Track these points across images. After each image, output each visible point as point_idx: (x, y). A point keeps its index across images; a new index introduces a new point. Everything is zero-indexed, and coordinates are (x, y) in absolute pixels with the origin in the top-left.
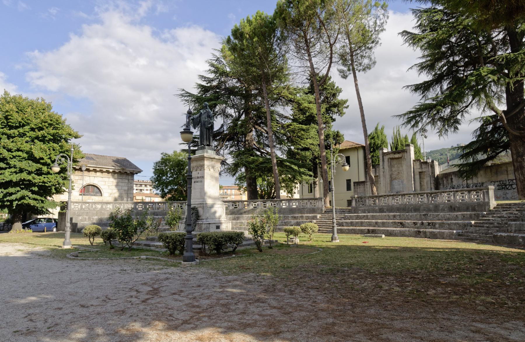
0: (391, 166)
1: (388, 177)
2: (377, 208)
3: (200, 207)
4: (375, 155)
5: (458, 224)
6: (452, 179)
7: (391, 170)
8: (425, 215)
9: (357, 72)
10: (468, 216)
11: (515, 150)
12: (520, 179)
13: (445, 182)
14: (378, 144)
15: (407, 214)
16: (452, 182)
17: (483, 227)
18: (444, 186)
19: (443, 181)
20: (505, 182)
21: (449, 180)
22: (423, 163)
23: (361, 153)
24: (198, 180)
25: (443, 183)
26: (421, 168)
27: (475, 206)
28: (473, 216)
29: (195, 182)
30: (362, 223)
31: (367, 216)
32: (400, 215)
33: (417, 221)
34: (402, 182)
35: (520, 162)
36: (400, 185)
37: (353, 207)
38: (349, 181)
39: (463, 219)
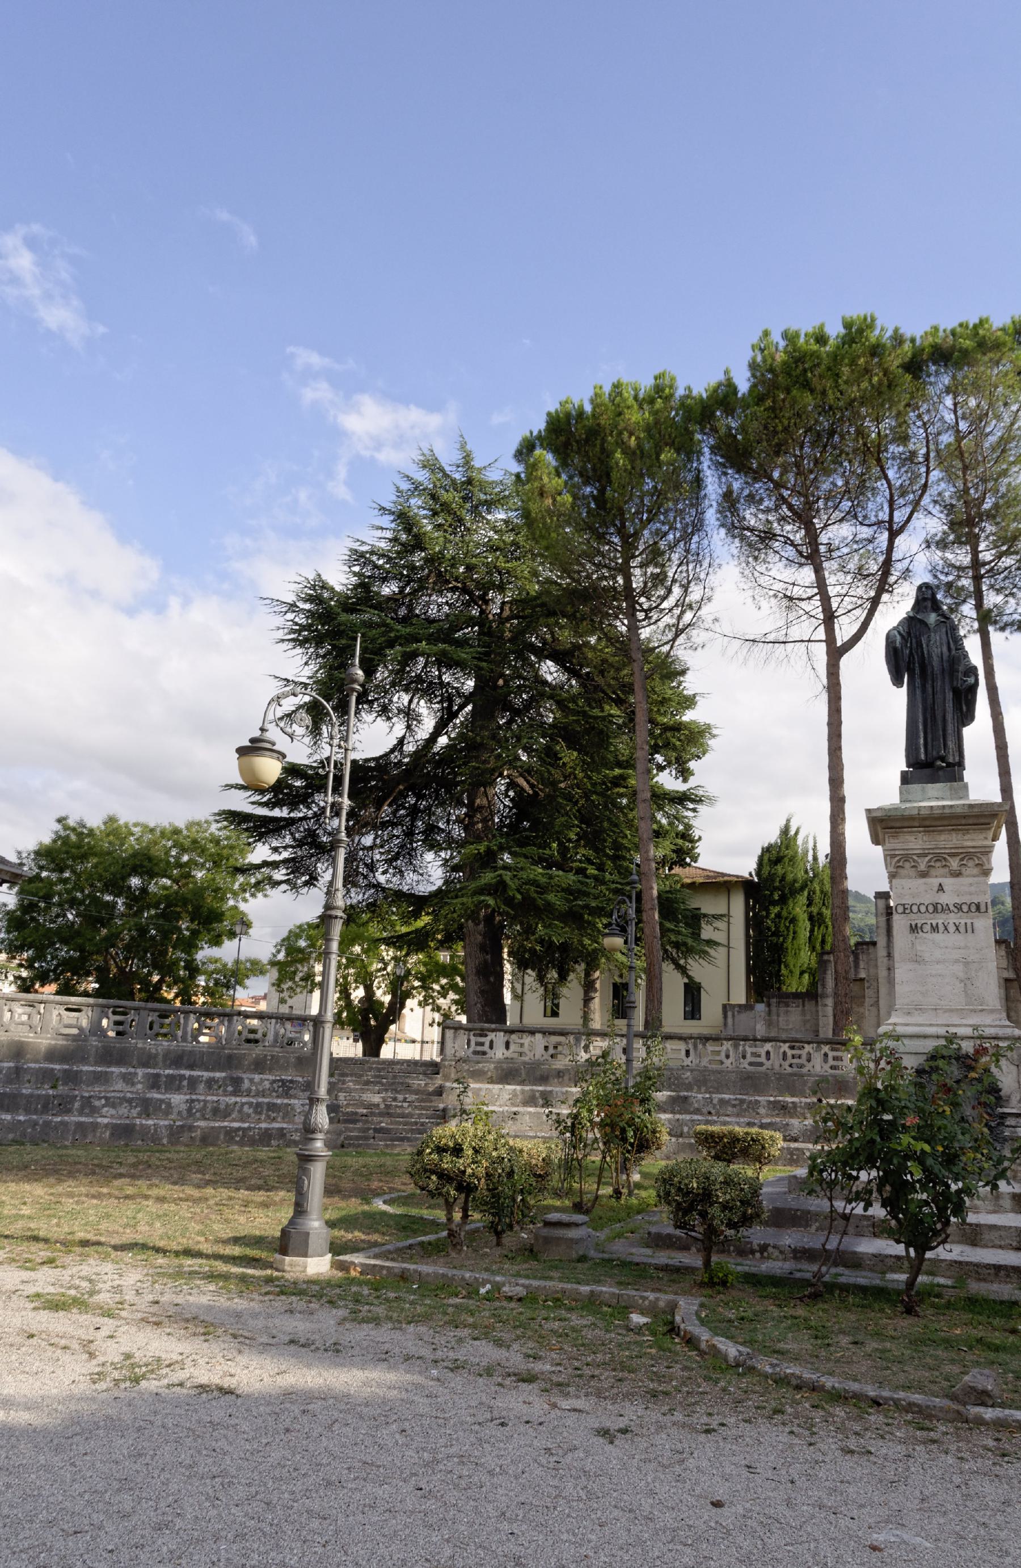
4: (784, 913)
14: (795, 881)
23: (738, 905)
24: (939, 919)
29: (914, 929)
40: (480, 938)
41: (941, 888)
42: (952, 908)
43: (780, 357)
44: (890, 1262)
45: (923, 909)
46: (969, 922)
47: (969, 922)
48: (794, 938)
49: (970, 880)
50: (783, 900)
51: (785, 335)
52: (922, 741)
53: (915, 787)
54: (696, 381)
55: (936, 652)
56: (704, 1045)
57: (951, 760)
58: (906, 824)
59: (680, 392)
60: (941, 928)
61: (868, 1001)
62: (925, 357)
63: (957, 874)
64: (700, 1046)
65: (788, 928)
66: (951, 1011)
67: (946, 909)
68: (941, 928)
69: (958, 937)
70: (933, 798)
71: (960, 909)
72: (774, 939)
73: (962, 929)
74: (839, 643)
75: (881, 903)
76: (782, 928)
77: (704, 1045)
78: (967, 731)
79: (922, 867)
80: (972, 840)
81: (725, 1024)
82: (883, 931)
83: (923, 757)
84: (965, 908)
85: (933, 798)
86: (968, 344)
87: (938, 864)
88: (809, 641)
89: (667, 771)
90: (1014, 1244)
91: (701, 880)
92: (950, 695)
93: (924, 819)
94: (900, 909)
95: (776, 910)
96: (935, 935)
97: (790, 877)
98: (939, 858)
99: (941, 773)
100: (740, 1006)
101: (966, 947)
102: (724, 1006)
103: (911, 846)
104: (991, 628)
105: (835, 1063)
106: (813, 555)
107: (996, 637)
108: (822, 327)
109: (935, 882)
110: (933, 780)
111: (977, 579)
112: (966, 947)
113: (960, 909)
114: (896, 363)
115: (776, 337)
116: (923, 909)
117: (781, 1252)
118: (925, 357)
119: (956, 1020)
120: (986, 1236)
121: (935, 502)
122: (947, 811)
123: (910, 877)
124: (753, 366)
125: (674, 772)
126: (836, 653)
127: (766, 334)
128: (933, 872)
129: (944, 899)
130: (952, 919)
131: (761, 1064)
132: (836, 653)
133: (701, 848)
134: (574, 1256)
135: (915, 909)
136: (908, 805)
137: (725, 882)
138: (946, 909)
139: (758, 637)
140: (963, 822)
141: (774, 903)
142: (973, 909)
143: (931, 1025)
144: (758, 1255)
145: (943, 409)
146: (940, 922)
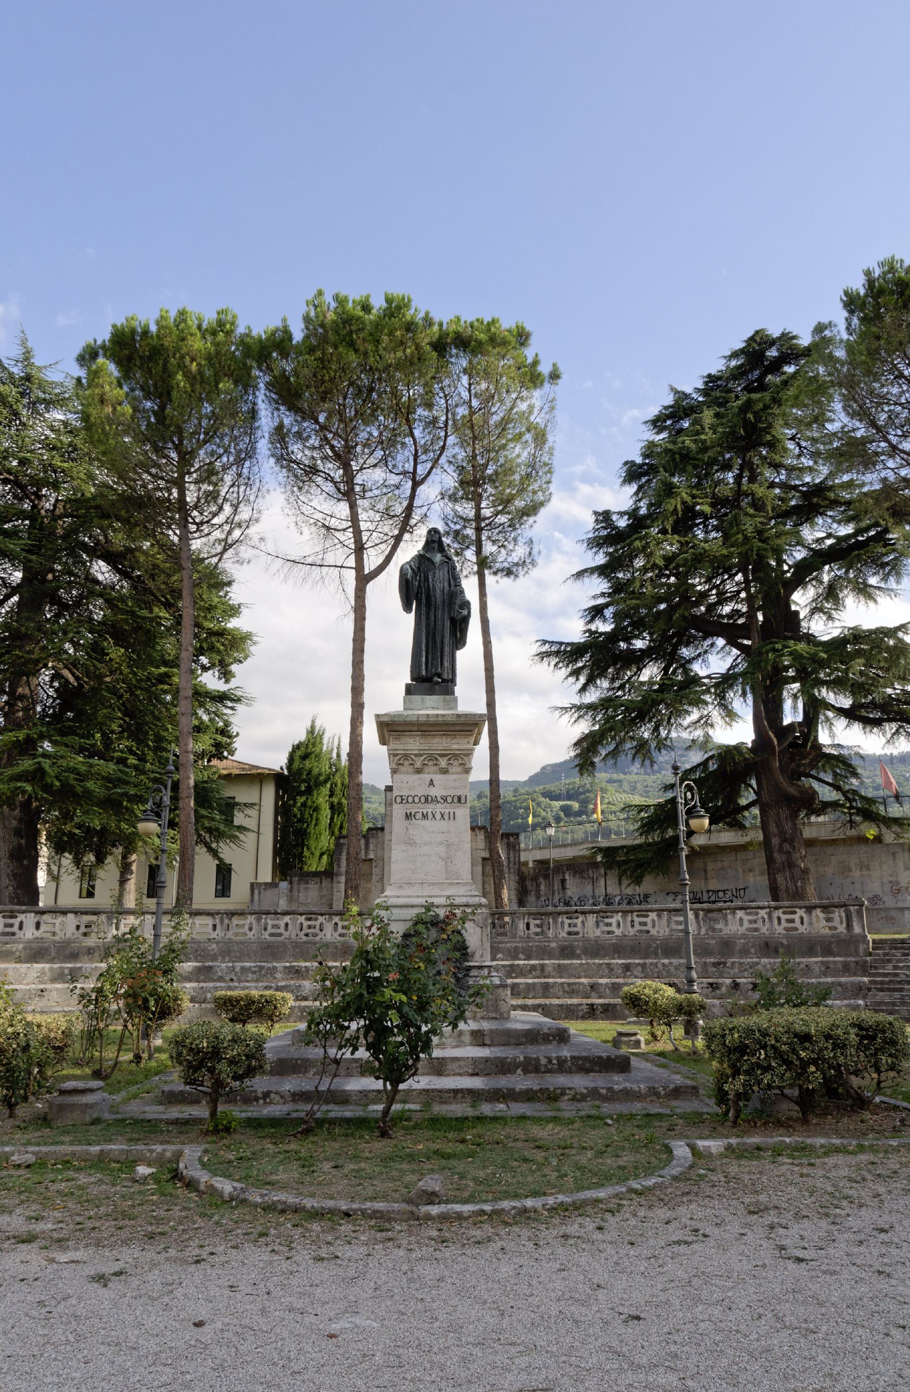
2: (553, 945)
4: (309, 803)
5: (840, 984)
6: (563, 881)
8: (719, 964)
10: (840, 966)
11: (777, 826)
12: (787, 890)
13: (542, 887)
14: (320, 774)
15: (666, 961)
16: (564, 888)
17: (901, 990)
18: (538, 897)
19: (538, 886)
20: (699, 895)
21: (557, 885)
23: (269, 794)
24: (429, 809)
25: (538, 890)
27: (831, 943)
28: (853, 965)
29: (408, 816)
30: (546, 986)
31: (543, 967)
32: (643, 966)
33: (720, 981)
35: (788, 853)
39: (825, 974)
40: (14, 823)
41: (431, 783)
43: (331, 316)
44: (371, 1096)
45: (417, 800)
46: (452, 811)
47: (452, 811)
48: (316, 825)
49: (455, 777)
50: (309, 791)
51: (336, 298)
53: (417, 698)
54: (256, 322)
55: (439, 586)
56: (230, 919)
58: (407, 728)
59: (241, 330)
60: (430, 816)
62: (449, 341)
63: (445, 771)
64: (226, 921)
65: (311, 816)
66: (434, 884)
67: (435, 800)
68: (430, 816)
69: (443, 823)
70: (430, 707)
71: (445, 801)
72: (299, 825)
73: (446, 817)
74: (366, 572)
76: (307, 816)
78: (459, 654)
79: (418, 765)
80: (457, 744)
81: (252, 901)
83: (424, 673)
84: (449, 800)
85: (430, 707)
86: (482, 336)
87: (431, 763)
88: (342, 567)
89: (211, 672)
90: (470, 1071)
92: (448, 624)
93: (423, 725)
94: (399, 800)
95: (303, 799)
96: (425, 822)
97: (316, 771)
98: (432, 758)
99: (437, 687)
100: (266, 884)
101: (449, 832)
102: (252, 885)
103: (410, 747)
104: (486, 572)
105: (344, 931)
106: (348, 492)
107: (490, 579)
108: (368, 298)
109: (427, 777)
110: (431, 693)
111: (479, 530)
112: (449, 832)
113: (445, 801)
114: (427, 340)
115: (328, 298)
116: (417, 800)
117: (282, 1097)
118: (449, 341)
120: (450, 1066)
121: (450, 462)
122: (440, 719)
123: (408, 773)
124: (307, 319)
125: (217, 674)
126: (363, 579)
127: (320, 293)
128: (426, 769)
129: (433, 792)
130: (439, 808)
131: (280, 935)
132: (363, 579)
133: (238, 744)
134: (88, 1119)
135: (410, 800)
136: (410, 712)
137: (259, 774)
138: (435, 800)
141: (301, 794)
144: (261, 1101)
145: (459, 387)
146: (430, 811)
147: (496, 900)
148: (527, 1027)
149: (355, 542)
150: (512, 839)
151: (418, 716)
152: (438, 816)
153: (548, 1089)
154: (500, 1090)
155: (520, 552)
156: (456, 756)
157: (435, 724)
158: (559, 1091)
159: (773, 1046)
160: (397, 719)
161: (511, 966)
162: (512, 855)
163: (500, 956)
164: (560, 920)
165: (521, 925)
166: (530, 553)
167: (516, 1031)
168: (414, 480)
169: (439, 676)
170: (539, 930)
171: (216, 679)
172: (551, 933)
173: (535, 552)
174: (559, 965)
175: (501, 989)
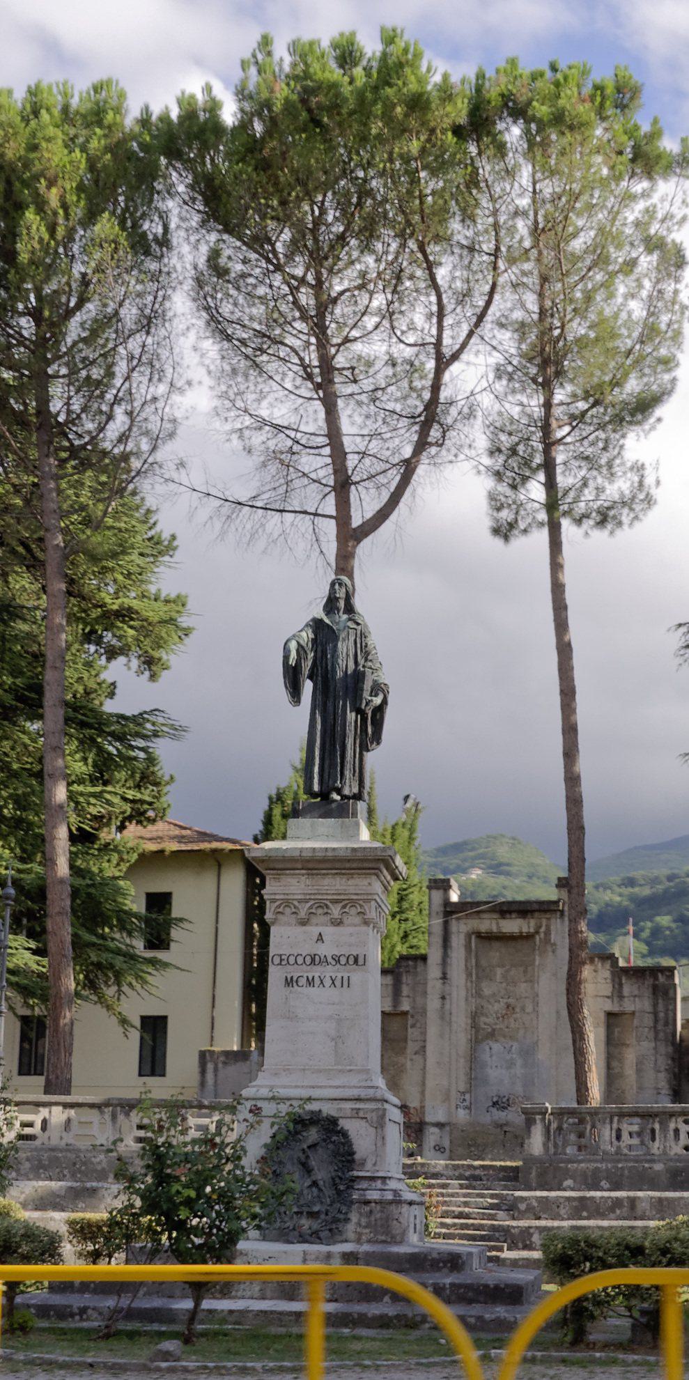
0: (478, 974)
1: (461, 1020)
2: (658, 1167)
3: (356, 1115)
7: (479, 994)
9: (565, 523)
22: (625, 971)
24: (316, 972)
26: (618, 993)
29: (289, 982)
31: (633, 1202)
34: (528, 1053)
36: (510, 1064)
37: (530, 1160)
38: (154, 1027)
41: (320, 938)
42: (330, 959)
43: (282, 92)
45: (300, 960)
49: (351, 929)
52: (316, 769)
55: (341, 662)
56: (127, 1114)
57: (346, 792)
58: (289, 866)
60: (317, 981)
61: (411, 1047)
63: (338, 923)
64: (121, 1117)
66: (320, 1071)
67: (324, 961)
68: (317, 981)
73: (338, 983)
75: (437, 896)
77: (127, 1114)
78: (370, 757)
81: (203, 1084)
82: (437, 940)
84: (343, 960)
87: (320, 911)
89: (122, 660)
91: (174, 846)
93: (308, 861)
94: (277, 960)
96: (311, 989)
100: (228, 1054)
102: (203, 1055)
103: (293, 890)
108: (353, 34)
109: (314, 930)
114: (447, 123)
116: (300, 960)
117: (100, 1314)
119: (322, 1080)
121: (502, 326)
122: (330, 854)
123: (290, 925)
125: (135, 663)
126: (351, 537)
128: (314, 920)
129: (324, 950)
130: (329, 972)
132: (351, 537)
135: (292, 960)
138: (324, 961)
139: (242, 500)
140: (348, 865)
142: (351, 961)
143: (296, 1087)
144: (77, 1318)
145: (518, 184)
147: (578, 1090)
148: (416, 1250)
149: (335, 472)
150: (661, 979)
151: (301, 850)
152: (328, 982)
153: (405, 1315)
154: (350, 1314)
155: (621, 486)
156: (353, 903)
157: (324, 860)
158: (419, 1319)
159: (599, 1258)
160: (272, 854)
161: (582, 1199)
162: (661, 1007)
163: (569, 1182)
164: (672, 1126)
165: (607, 1133)
166: (641, 484)
167: (398, 1254)
168: (439, 357)
169: (339, 791)
170: (635, 1141)
171: (132, 673)
172: (656, 1147)
173: (650, 480)
174: (660, 1200)
175: (393, 1207)
